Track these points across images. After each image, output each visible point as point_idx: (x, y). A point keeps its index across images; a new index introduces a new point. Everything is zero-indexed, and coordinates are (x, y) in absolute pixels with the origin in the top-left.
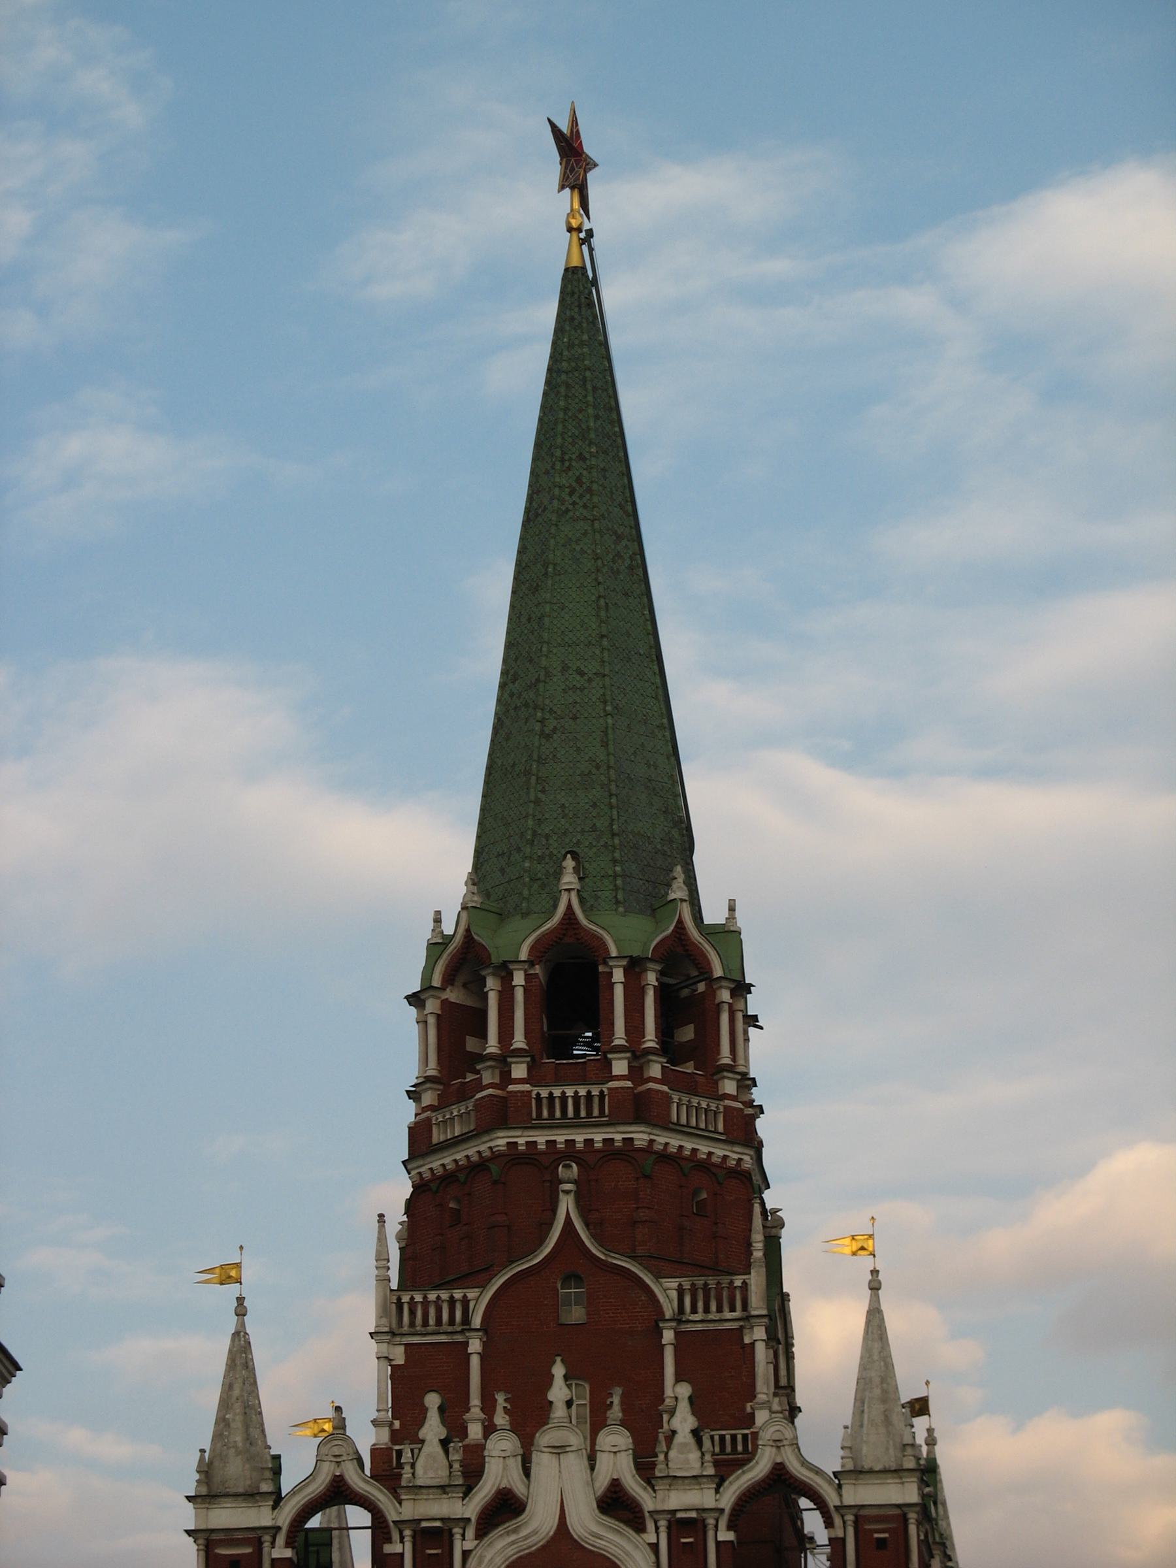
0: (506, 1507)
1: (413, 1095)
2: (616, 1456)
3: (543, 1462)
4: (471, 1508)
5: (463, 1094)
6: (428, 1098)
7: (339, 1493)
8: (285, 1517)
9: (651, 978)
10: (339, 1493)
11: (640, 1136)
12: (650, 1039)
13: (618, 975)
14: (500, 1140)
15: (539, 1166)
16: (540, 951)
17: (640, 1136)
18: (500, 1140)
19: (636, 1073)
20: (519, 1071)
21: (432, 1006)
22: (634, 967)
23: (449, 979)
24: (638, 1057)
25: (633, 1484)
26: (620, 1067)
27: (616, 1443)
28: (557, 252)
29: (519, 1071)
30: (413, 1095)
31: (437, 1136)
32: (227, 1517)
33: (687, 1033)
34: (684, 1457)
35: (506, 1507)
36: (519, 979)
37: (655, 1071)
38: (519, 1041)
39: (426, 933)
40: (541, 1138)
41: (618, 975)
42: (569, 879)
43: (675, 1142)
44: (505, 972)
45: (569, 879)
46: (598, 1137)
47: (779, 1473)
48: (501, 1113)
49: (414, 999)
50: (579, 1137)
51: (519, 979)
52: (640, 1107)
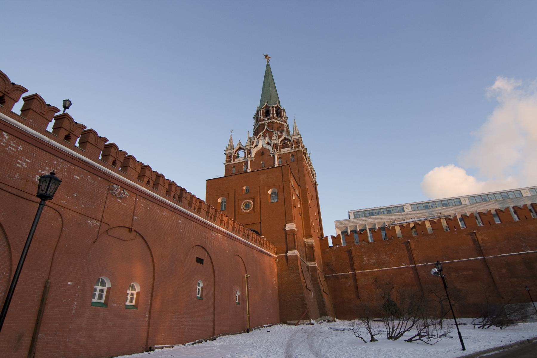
0: (256, 146)
2: (267, 139)
3: (260, 142)
7: (240, 149)
8: (235, 151)
10: (240, 149)
11: (274, 120)
14: (260, 123)
15: (264, 125)
17: (274, 120)
18: (260, 123)
20: (262, 117)
22: (273, 107)
24: (273, 114)
25: (270, 142)
26: (271, 115)
27: (267, 139)
29: (262, 117)
34: (274, 138)
35: (256, 146)
37: (275, 115)
40: (264, 122)
43: (277, 121)
46: (269, 121)
47: (285, 139)
52: (274, 118)
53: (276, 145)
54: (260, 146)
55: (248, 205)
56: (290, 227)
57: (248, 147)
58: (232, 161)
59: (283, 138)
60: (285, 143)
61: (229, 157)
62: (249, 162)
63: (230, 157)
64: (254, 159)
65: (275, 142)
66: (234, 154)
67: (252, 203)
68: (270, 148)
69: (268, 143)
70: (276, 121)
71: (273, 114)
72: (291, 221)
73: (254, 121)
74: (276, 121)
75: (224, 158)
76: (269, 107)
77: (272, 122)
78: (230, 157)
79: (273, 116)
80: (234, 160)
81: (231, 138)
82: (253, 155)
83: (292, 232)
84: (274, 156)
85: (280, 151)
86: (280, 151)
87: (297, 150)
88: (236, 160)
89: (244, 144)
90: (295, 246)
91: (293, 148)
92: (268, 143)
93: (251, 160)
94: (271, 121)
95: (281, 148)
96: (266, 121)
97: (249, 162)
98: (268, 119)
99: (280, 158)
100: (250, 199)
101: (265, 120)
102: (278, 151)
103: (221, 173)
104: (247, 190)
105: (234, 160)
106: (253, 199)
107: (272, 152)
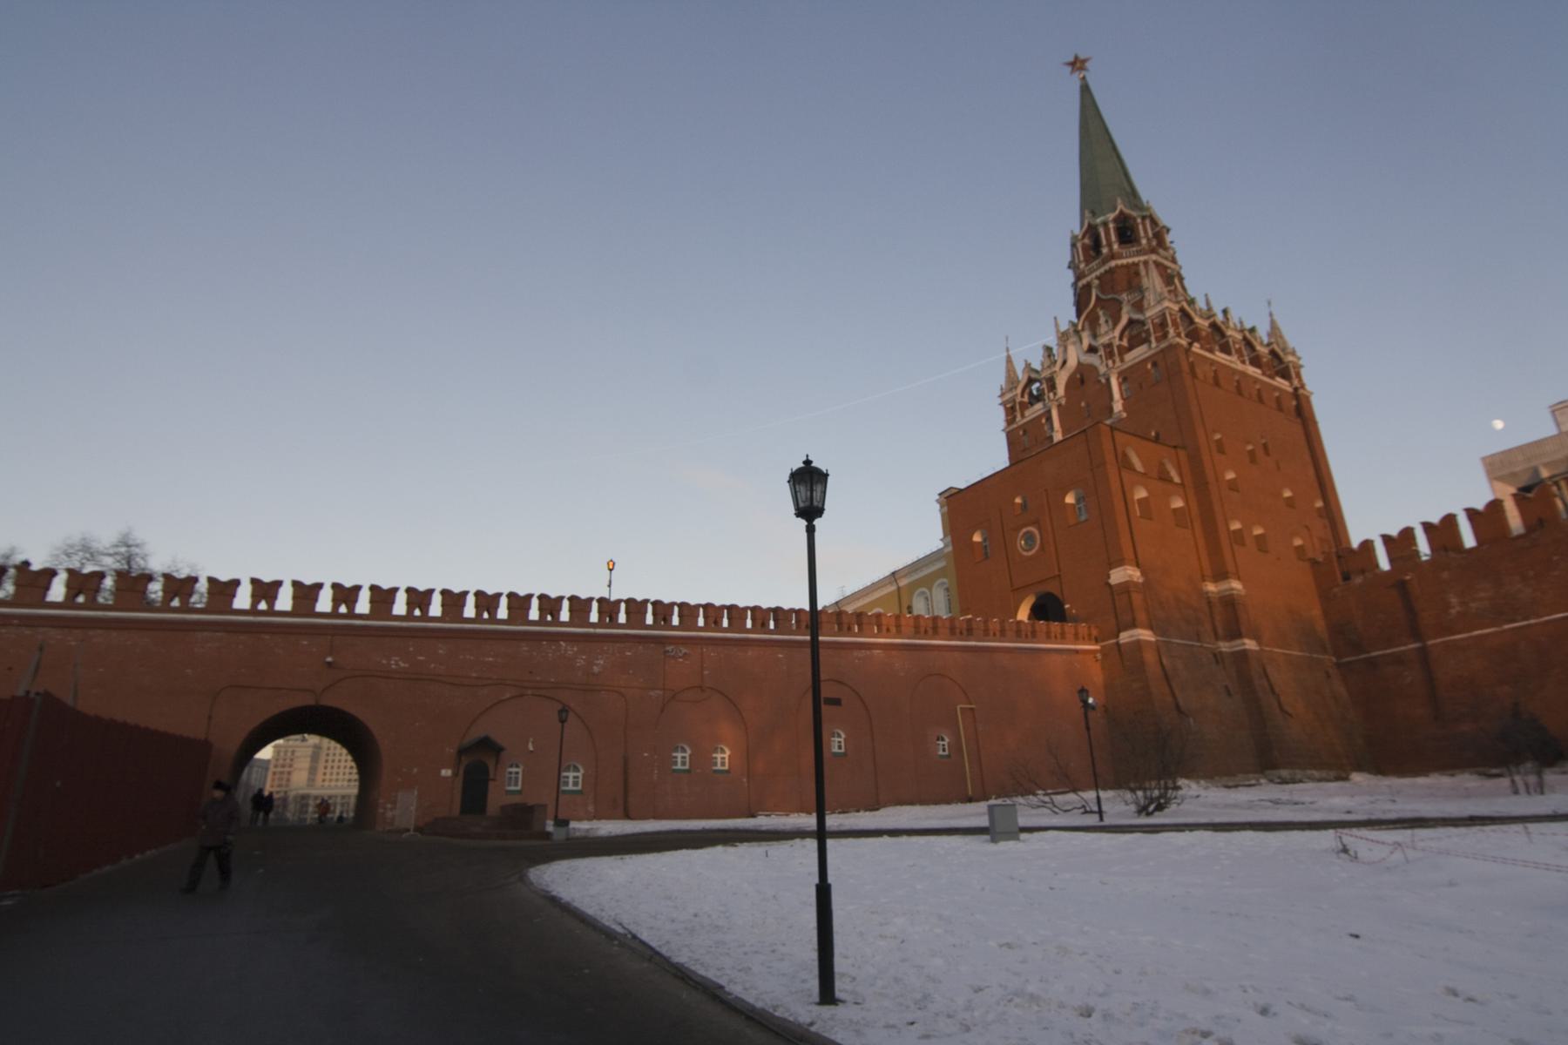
0: (1065, 362)
4: (1057, 368)
8: (1019, 390)
9: (1111, 226)
10: (1031, 381)
11: (1113, 263)
12: (1113, 238)
17: (1113, 263)
18: (1080, 284)
20: (1082, 266)
25: (1094, 343)
26: (1105, 250)
28: (1074, 82)
29: (1082, 266)
32: (1008, 396)
34: (1103, 328)
35: (1065, 362)
36: (1079, 245)
37: (1116, 247)
43: (1124, 261)
46: (1102, 270)
47: (1131, 322)
50: (1098, 273)
52: (1113, 256)
53: (1109, 346)
54: (1072, 362)
55: (1029, 537)
56: (1118, 576)
57: (1046, 374)
58: (1019, 418)
59: (1124, 321)
60: (1136, 334)
61: (1011, 411)
62: (1055, 414)
63: (1013, 408)
64: (1063, 402)
65: (1104, 340)
66: (1019, 399)
67: (1036, 532)
68: (1093, 359)
69: (1092, 350)
70: (1119, 262)
71: (1110, 245)
72: (1120, 562)
74: (1119, 262)
75: (1000, 414)
78: (1013, 408)
80: (1023, 416)
81: (1009, 360)
82: (1061, 390)
83: (1126, 587)
84: (1108, 380)
85: (1122, 360)
86: (1122, 360)
87: (1163, 345)
88: (1027, 413)
89: (1037, 366)
90: (1134, 620)
91: (1154, 345)
92: (1092, 350)
93: (1059, 406)
94: (1106, 267)
95: (1123, 351)
97: (1055, 414)
99: (1124, 377)
100: (1032, 524)
101: (1091, 272)
102: (1118, 363)
103: (991, 456)
104: (1024, 506)
105: (1023, 416)
106: (1036, 523)
107: (1102, 369)
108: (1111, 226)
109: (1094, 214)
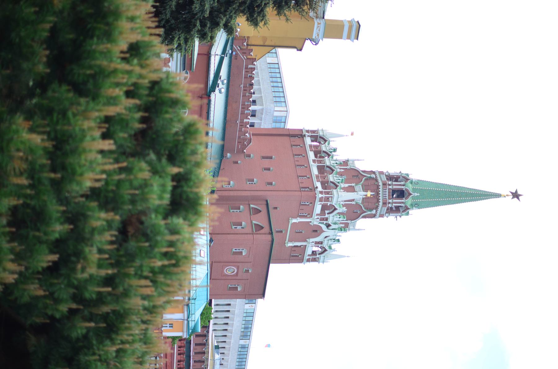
1: (387, 172)
5: (387, 179)
6: (387, 174)
9: (402, 205)
11: (381, 204)
13: (403, 201)
14: (381, 184)
16: (406, 189)
17: (381, 204)
18: (381, 184)
19: (389, 203)
20: (390, 187)
21: (399, 174)
23: (403, 177)
26: (390, 201)
29: (390, 187)
30: (387, 172)
31: (382, 176)
33: (394, 209)
37: (390, 205)
38: (394, 187)
39: (409, 173)
40: (381, 190)
41: (403, 201)
42: (416, 194)
43: (380, 208)
44: (404, 185)
45: (416, 194)
48: (384, 184)
49: (400, 172)
50: (381, 195)
51: (403, 187)
52: (384, 204)
73: (393, 170)
76: (406, 199)
77: (378, 201)
79: (389, 203)
94: (381, 201)
96: (383, 194)
98: (384, 195)
108: (402, 205)
109: (414, 198)
